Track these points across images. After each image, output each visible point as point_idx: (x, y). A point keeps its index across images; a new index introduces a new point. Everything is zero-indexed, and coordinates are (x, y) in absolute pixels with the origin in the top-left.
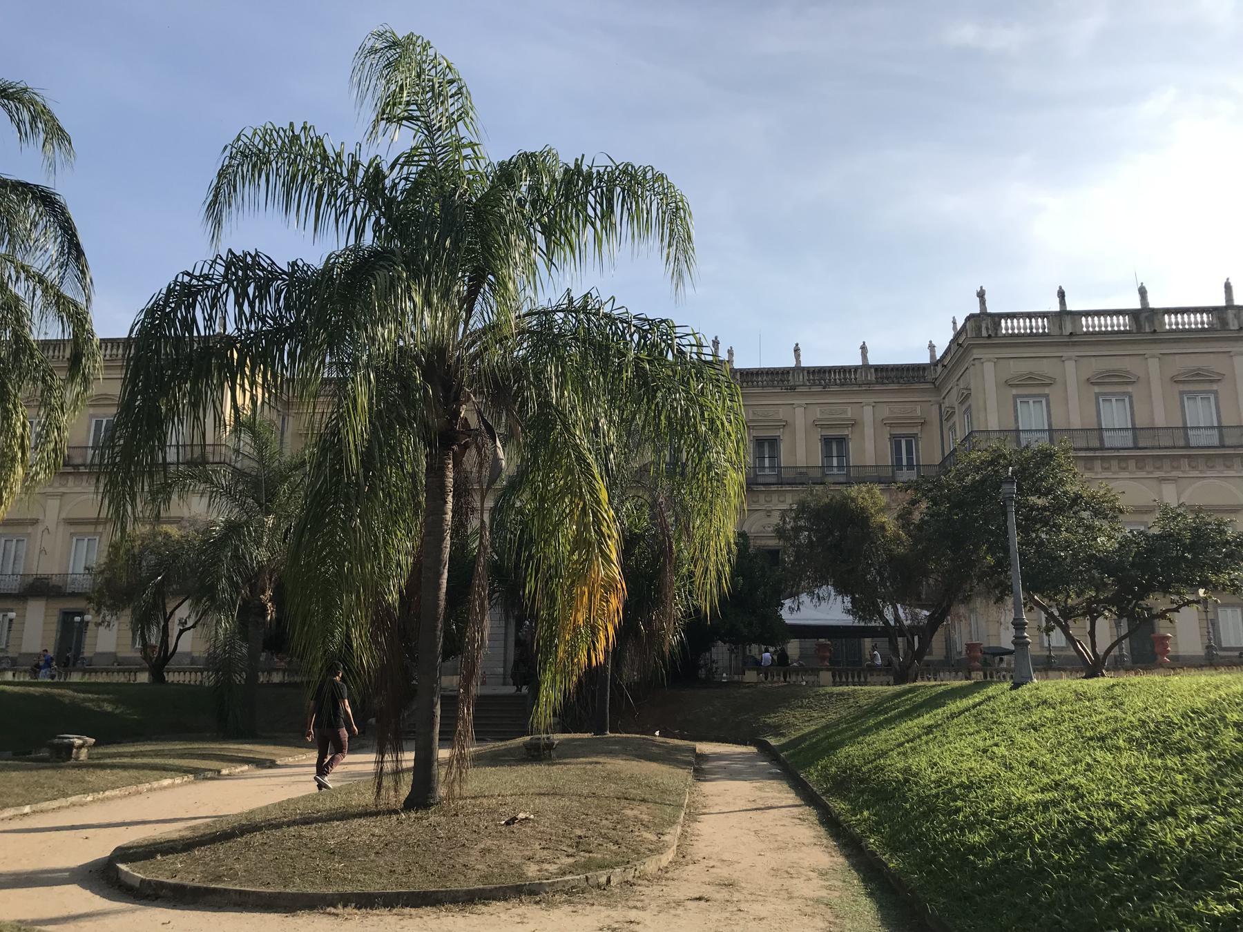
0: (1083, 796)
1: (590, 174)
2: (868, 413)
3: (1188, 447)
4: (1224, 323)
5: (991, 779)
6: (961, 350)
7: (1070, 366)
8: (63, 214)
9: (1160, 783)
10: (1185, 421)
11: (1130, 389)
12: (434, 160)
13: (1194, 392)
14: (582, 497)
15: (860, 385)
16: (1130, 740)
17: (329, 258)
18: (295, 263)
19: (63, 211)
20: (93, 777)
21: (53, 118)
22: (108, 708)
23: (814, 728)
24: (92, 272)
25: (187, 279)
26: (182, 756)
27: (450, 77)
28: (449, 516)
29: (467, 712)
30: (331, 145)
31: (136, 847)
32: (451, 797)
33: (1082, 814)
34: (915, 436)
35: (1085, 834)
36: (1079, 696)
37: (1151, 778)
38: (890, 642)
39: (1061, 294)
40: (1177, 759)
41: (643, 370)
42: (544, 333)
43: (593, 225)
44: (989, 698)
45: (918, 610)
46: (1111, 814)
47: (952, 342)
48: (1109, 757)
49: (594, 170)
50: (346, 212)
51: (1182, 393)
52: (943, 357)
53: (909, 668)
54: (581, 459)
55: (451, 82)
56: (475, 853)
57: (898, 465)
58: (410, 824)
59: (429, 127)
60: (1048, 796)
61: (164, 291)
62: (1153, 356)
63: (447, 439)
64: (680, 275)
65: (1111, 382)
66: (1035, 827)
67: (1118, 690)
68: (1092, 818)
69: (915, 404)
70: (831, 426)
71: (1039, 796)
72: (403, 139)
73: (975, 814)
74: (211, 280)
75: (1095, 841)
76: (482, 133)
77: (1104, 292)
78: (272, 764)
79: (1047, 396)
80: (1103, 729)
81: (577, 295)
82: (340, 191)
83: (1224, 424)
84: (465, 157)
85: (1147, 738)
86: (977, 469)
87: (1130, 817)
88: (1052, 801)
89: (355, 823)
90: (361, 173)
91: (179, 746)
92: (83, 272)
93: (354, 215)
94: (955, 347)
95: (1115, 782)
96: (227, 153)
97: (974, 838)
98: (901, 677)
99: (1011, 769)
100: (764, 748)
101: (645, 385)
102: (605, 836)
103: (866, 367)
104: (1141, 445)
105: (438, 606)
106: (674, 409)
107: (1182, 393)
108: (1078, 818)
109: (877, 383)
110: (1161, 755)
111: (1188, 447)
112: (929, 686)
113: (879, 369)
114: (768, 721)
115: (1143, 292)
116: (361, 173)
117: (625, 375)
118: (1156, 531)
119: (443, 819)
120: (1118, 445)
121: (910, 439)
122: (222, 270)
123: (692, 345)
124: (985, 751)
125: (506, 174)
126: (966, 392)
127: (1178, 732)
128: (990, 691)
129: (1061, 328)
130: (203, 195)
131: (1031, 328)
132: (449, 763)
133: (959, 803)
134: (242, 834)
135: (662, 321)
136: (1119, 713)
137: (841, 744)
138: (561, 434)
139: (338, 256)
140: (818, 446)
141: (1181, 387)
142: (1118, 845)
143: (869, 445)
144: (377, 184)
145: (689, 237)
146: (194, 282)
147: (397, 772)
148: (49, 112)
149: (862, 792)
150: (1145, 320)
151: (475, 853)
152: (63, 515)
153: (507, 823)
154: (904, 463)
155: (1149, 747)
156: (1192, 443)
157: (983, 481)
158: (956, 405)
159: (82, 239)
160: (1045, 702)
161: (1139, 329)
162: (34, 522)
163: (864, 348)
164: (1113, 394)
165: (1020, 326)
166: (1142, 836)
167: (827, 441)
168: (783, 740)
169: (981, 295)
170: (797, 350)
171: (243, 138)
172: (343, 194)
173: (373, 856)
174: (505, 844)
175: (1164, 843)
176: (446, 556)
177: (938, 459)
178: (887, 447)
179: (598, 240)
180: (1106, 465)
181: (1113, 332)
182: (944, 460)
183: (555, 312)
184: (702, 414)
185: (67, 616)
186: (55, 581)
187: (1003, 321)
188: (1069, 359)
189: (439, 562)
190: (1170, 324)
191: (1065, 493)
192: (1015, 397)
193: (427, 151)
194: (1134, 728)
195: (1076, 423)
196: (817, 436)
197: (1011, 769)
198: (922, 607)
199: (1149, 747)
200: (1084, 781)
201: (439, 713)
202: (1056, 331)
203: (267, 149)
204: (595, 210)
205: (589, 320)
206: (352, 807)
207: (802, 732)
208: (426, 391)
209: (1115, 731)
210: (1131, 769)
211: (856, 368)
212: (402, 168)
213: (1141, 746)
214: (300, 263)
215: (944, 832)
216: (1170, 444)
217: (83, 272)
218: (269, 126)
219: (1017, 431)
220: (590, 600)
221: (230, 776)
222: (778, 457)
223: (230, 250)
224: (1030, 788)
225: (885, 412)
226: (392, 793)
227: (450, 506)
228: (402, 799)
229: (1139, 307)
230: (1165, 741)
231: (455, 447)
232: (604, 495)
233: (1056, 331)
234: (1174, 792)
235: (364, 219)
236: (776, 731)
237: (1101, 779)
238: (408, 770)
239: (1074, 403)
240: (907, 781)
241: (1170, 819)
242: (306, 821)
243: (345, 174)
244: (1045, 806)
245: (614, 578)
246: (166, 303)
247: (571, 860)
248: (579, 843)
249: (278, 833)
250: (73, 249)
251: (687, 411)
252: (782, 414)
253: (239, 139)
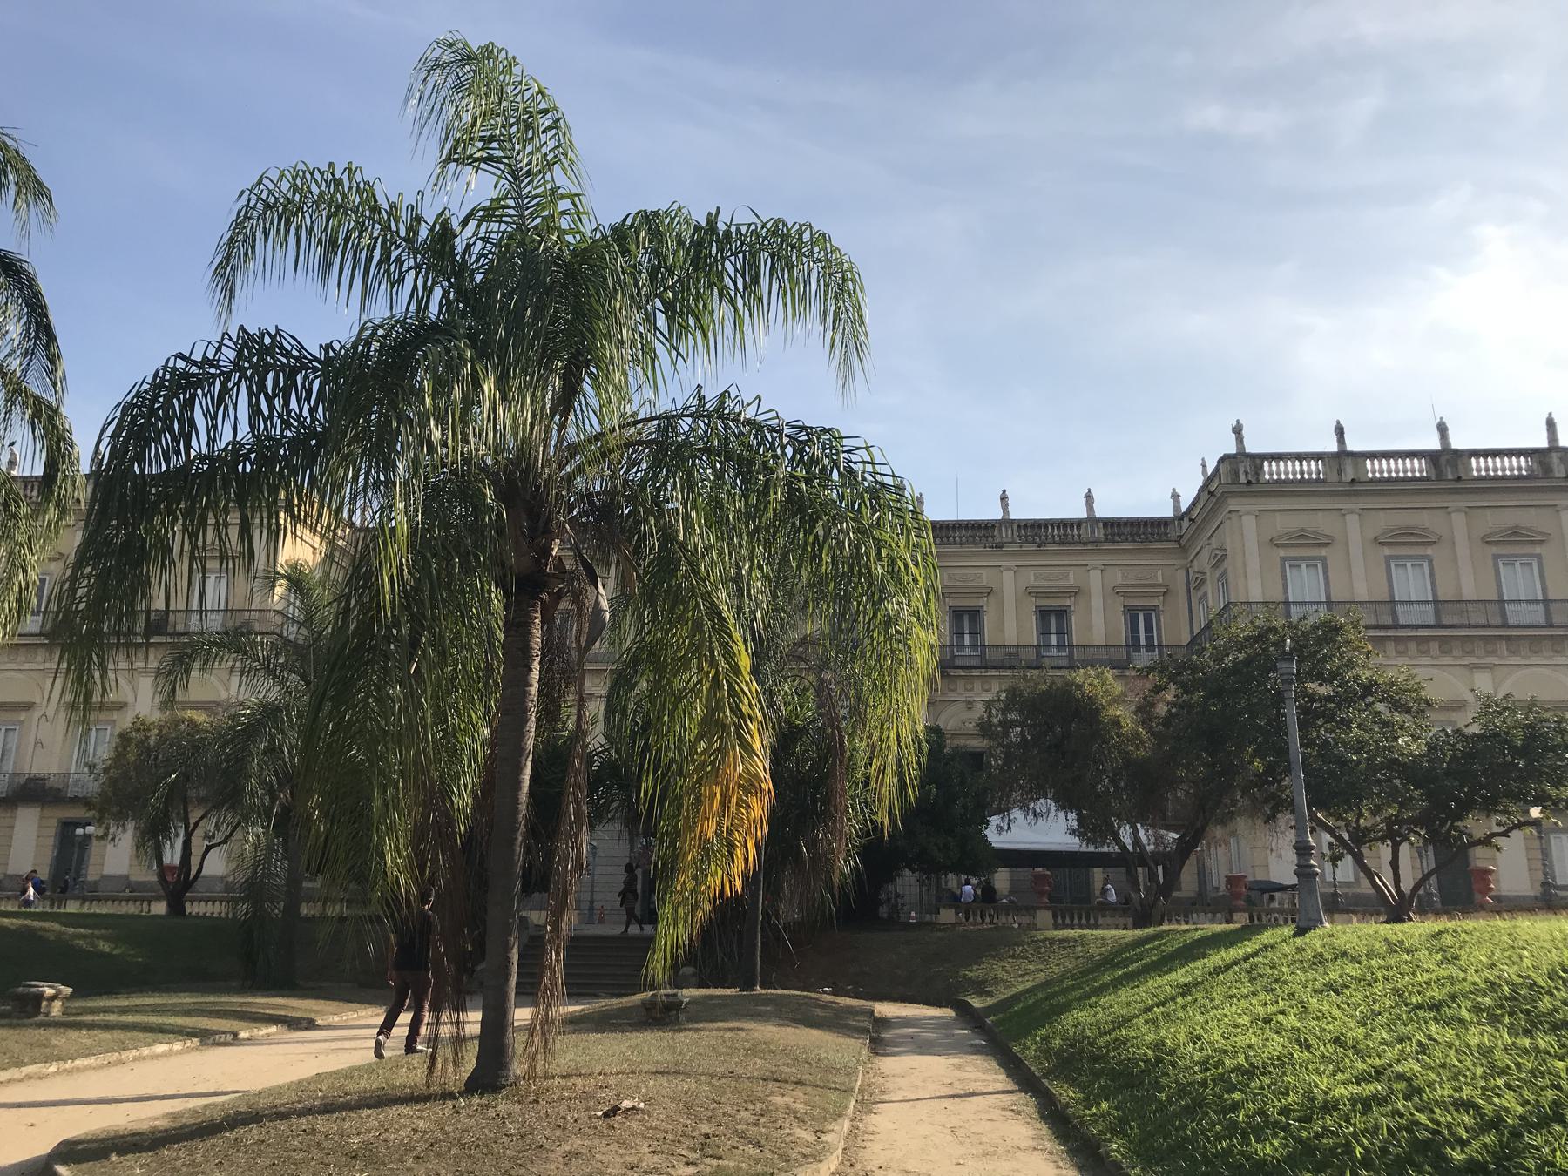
0: (1419, 1091)
1: (728, 234)
2: (1095, 578)
3: (1506, 626)
4: (1547, 470)
5: (1282, 1062)
6: (1214, 500)
7: (1352, 521)
8: (31, 286)
9: (1532, 1072)
10: (1500, 593)
11: (1429, 551)
12: (521, 216)
13: (1516, 556)
14: (713, 663)
15: (1085, 543)
16: (1477, 1009)
17: (363, 329)
18: (329, 346)
19: (32, 281)
20: (59, 1040)
21: (29, 168)
22: (105, 947)
23: (1030, 984)
24: (66, 364)
25: (181, 364)
26: (188, 1013)
27: (543, 106)
28: (534, 690)
29: (555, 958)
30: (384, 194)
31: (89, 1141)
32: (531, 1076)
33: (1422, 1118)
34: (1155, 608)
35: (1430, 1148)
36: (1393, 947)
37: (1518, 1065)
38: (1129, 872)
39: (1340, 431)
40: (1552, 1039)
41: (805, 499)
42: (668, 448)
43: (733, 302)
44: (1266, 947)
45: (1163, 832)
46: (1466, 1118)
47: (1201, 490)
48: (1450, 1034)
49: (733, 229)
50: (401, 280)
51: (1496, 557)
52: (1190, 509)
53: (1153, 906)
54: (715, 612)
55: (545, 112)
56: (557, 1157)
57: (1134, 645)
58: (470, 1116)
59: (514, 171)
60: (1369, 1089)
61: (149, 380)
62: (1458, 510)
63: (531, 586)
64: (849, 368)
65: (1405, 543)
66: (1355, 1135)
67: (1447, 940)
68: (1438, 1123)
69: (1154, 568)
70: (1047, 595)
71: (1354, 1089)
72: (480, 186)
73: (1261, 1112)
74: (217, 367)
75: (1447, 1160)
76: (585, 181)
77: (1394, 428)
78: (310, 1025)
79: (1324, 560)
80: (1436, 993)
81: (711, 394)
82: (394, 255)
83: (1551, 597)
84: (564, 213)
85: (1502, 1007)
86: (1241, 647)
87: (1496, 1123)
88: (1375, 1097)
89: (393, 1112)
90: (424, 232)
91: (187, 999)
92: (53, 363)
93: (415, 287)
94: (1205, 496)
95: (1465, 1068)
96: (244, 201)
97: (1267, 1149)
98: (1141, 921)
99: (1308, 1048)
100: (964, 1010)
101: (800, 507)
102: (742, 1135)
103: (1092, 521)
104: (1445, 622)
105: (517, 812)
106: (840, 544)
107: (1496, 557)
108: (1417, 1123)
109: (1106, 541)
110: (1527, 1032)
111: (1506, 626)
112: (1182, 931)
113: (1109, 523)
114: (970, 975)
115: (1442, 429)
116: (424, 232)
117: (773, 496)
118: (1475, 729)
119: (517, 1108)
120: (1415, 621)
121: (1150, 613)
122: (232, 355)
123: (864, 462)
124: (1267, 1021)
125: (621, 234)
126: (1220, 553)
127: (1547, 998)
128: (1266, 937)
129: (1339, 473)
130: (207, 252)
131: (1302, 473)
132: (530, 1029)
133: (1237, 1096)
134: (232, 1129)
135: (826, 431)
136: (1455, 971)
137: (1066, 1008)
138: (687, 577)
139: (375, 328)
140: (1032, 622)
141: (1494, 550)
142: (1482, 1167)
143: (1098, 621)
144: (444, 246)
145: (861, 317)
146: (194, 369)
147: (458, 1040)
148: (23, 159)
149: (1097, 1075)
150: (1446, 466)
151: (557, 1157)
153: (606, 1115)
154: (1143, 642)
155: (1507, 1020)
156: (1511, 621)
157: (1248, 662)
158: (1207, 570)
159: (55, 319)
160: (1344, 954)
161: (1440, 477)
162: (29, 707)
163: (1089, 496)
164: (1409, 557)
165: (1287, 470)
166: (1519, 1153)
167: (1043, 614)
168: (990, 1001)
169: (1238, 430)
170: (1004, 498)
171: (265, 181)
172: (398, 258)
173: (410, 1163)
174: (600, 1145)
175: (1552, 1165)
176: (530, 742)
177: (1185, 638)
178: (1121, 622)
179: (738, 321)
180: (1401, 648)
181: (1406, 479)
182: (1194, 639)
183: (680, 417)
184: (879, 553)
185: (67, 827)
186: (53, 782)
187: (1266, 464)
188: (1352, 512)
189: (520, 751)
190: (1479, 470)
191: (1356, 678)
192: (1284, 560)
193: (511, 203)
194: (1478, 991)
195: (1361, 592)
196: (1031, 605)
197: (1308, 1048)
198: (1169, 828)
199: (1507, 1020)
200: (1417, 1067)
201: (515, 957)
202: (1335, 478)
203: (297, 198)
204: (735, 283)
205: (726, 428)
206: (394, 1087)
207: (1013, 991)
208: (500, 515)
209: (1453, 997)
210: (1486, 1052)
211: (1080, 522)
212: (478, 226)
213: (1494, 1020)
214: (337, 346)
215: (1218, 1138)
216: (1483, 621)
217: (53, 363)
218: (301, 167)
219: (1287, 603)
220: (723, 804)
221: (250, 1041)
222: (981, 633)
223: (242, 328)
224: (1340, 1077)
225: (1117, 577)
226: (451, 1069)
227: (535, 675)
228: (466, 1076)
229: (1434, 444)
230: (1528, 1012)
231: (545, 596)
232: (745, 662)
233: (1335, 478)
234: (1558, 1087)
235: (429, 291)
236: (980, 988)
237: (1443, 1066)
238: (472, 1038)
240: (1159, 1060)
241: (1558, 1128)
242: (328, 1108)
243: (403, 233)
244: (1366, 1104)
245: (757, 776)
246: (155, 398)
247: (692, 1170)
248: (705, 1145)
249: (283, 1126)
250: (42, 332)
251: (858, 547)
252: (985, 578)
253: (260, 183)
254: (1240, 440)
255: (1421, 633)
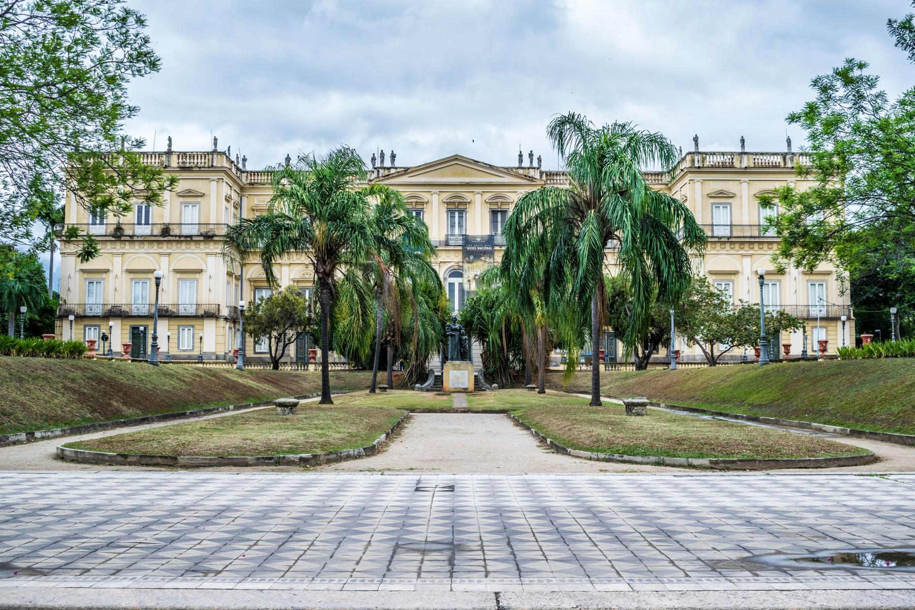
79: (730, 204)
115: (789, 142)
152: (125, 268)
169: (696, 139)
185: (135, 329)
186: (124, 308)
192: (713, 204)
195: (746, 222)
219: (712, 225)
229: (785, 150)
239: (745, 209)
254: (697, 145)
255: (769, 240)
